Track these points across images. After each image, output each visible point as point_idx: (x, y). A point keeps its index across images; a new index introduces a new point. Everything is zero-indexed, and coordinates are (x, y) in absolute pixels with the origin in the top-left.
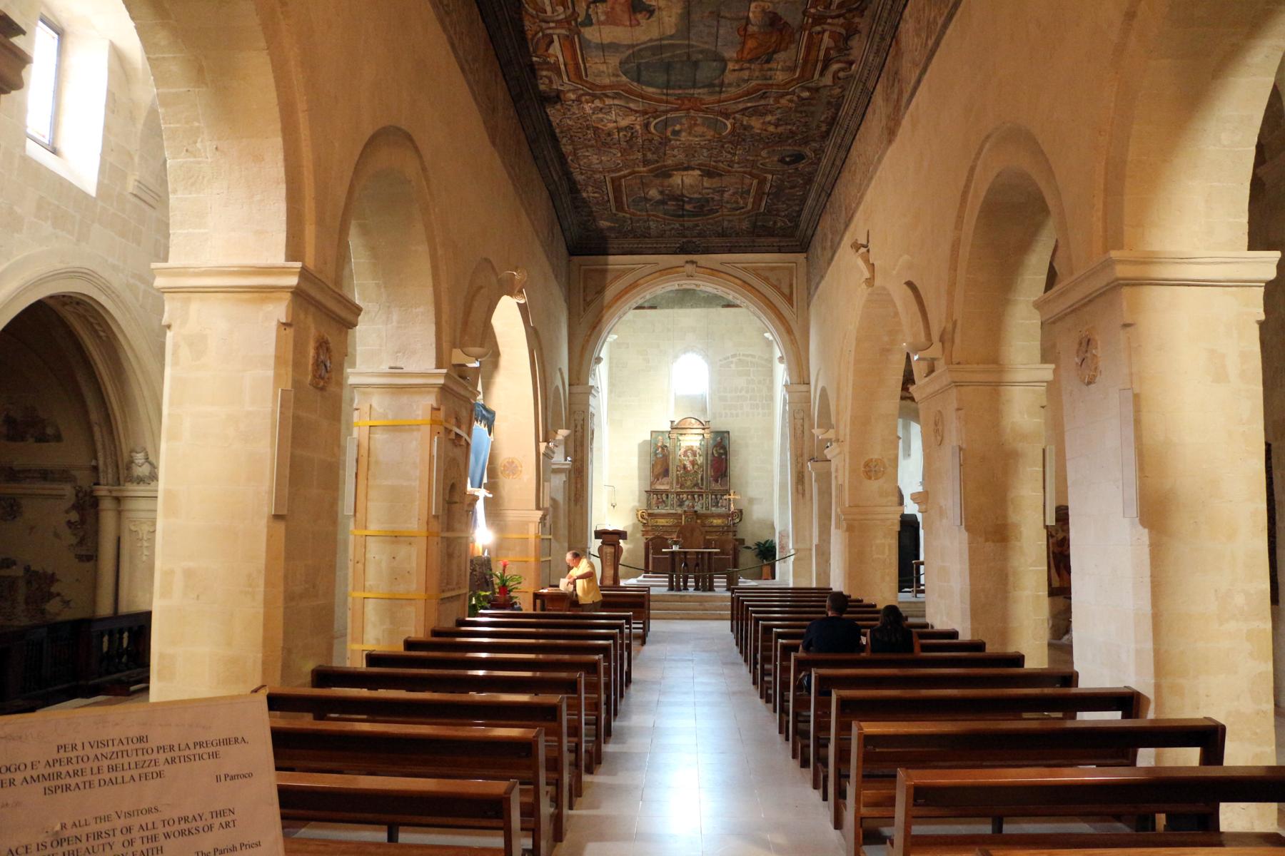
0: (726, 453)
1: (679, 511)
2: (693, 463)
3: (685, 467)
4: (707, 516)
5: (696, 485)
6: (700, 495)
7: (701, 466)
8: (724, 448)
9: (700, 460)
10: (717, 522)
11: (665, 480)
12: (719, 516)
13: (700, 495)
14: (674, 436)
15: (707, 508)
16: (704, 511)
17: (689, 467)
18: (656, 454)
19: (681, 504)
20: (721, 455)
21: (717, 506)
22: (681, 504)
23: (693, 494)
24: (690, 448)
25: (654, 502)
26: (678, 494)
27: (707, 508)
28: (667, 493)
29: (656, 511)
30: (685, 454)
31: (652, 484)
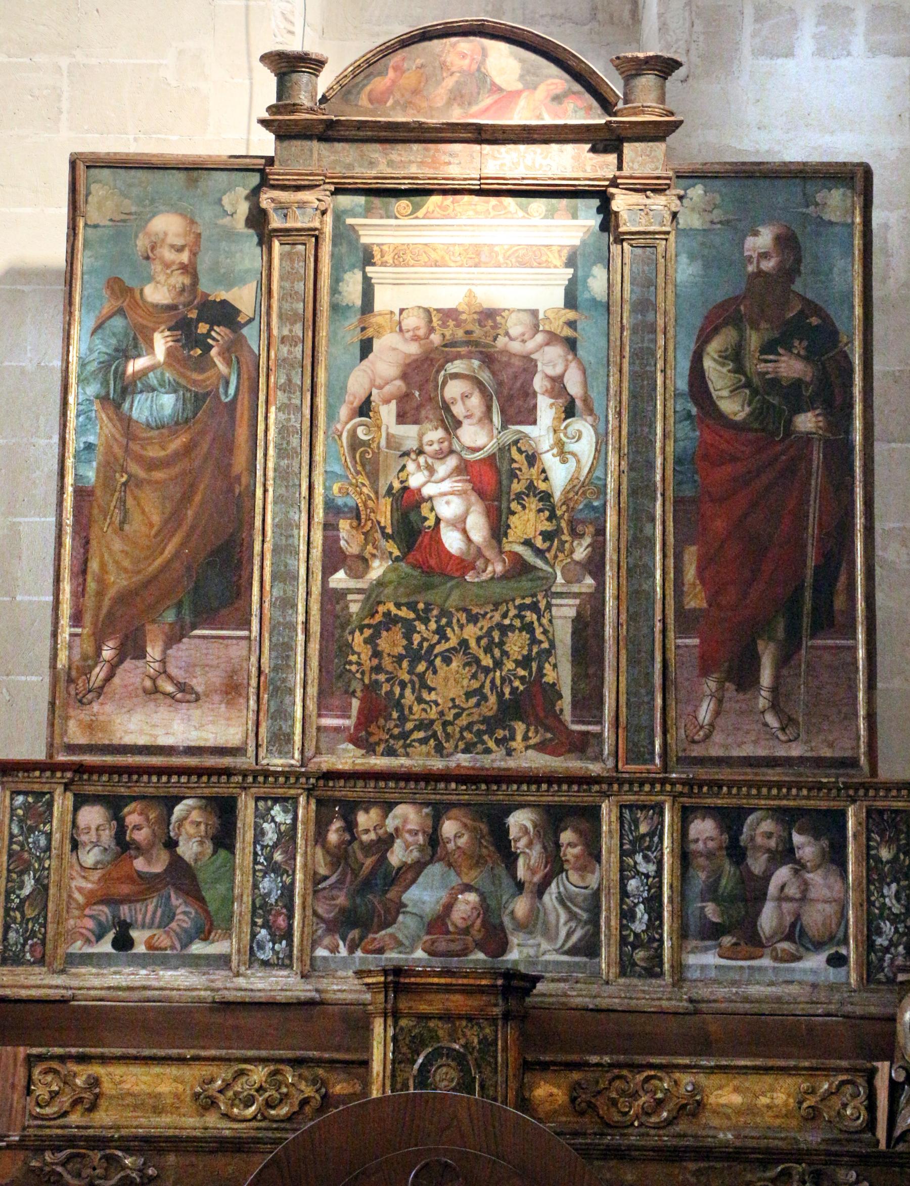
0: (832, 387)
1: (344, 978)
2: (497, 483)
3: (411, 525)
4: (635, 1040)
5: (528, 704)
6: (568, 811)
7: (573, 516)
8: (815, 334)
9: (567, 452)
10: (742, 1101)
11: (205, 653)
12: (763, 1038)
13: (568, 811)
14: (308, 209)
15: (641, 957)
16: (607, 986)
17: (456, 517)
18: (118, 391)
19: (365, 898)
20: (775, 402)
21: (738, 929)
22: (365, 898)
23: (486, 798)
24: (470, 344)
25: (81, 873)
26: (335, 796)
27: (641, 957)
28: (218, 785)
29: (106, 980)
30: (419, 391)
31: (71, 688)
